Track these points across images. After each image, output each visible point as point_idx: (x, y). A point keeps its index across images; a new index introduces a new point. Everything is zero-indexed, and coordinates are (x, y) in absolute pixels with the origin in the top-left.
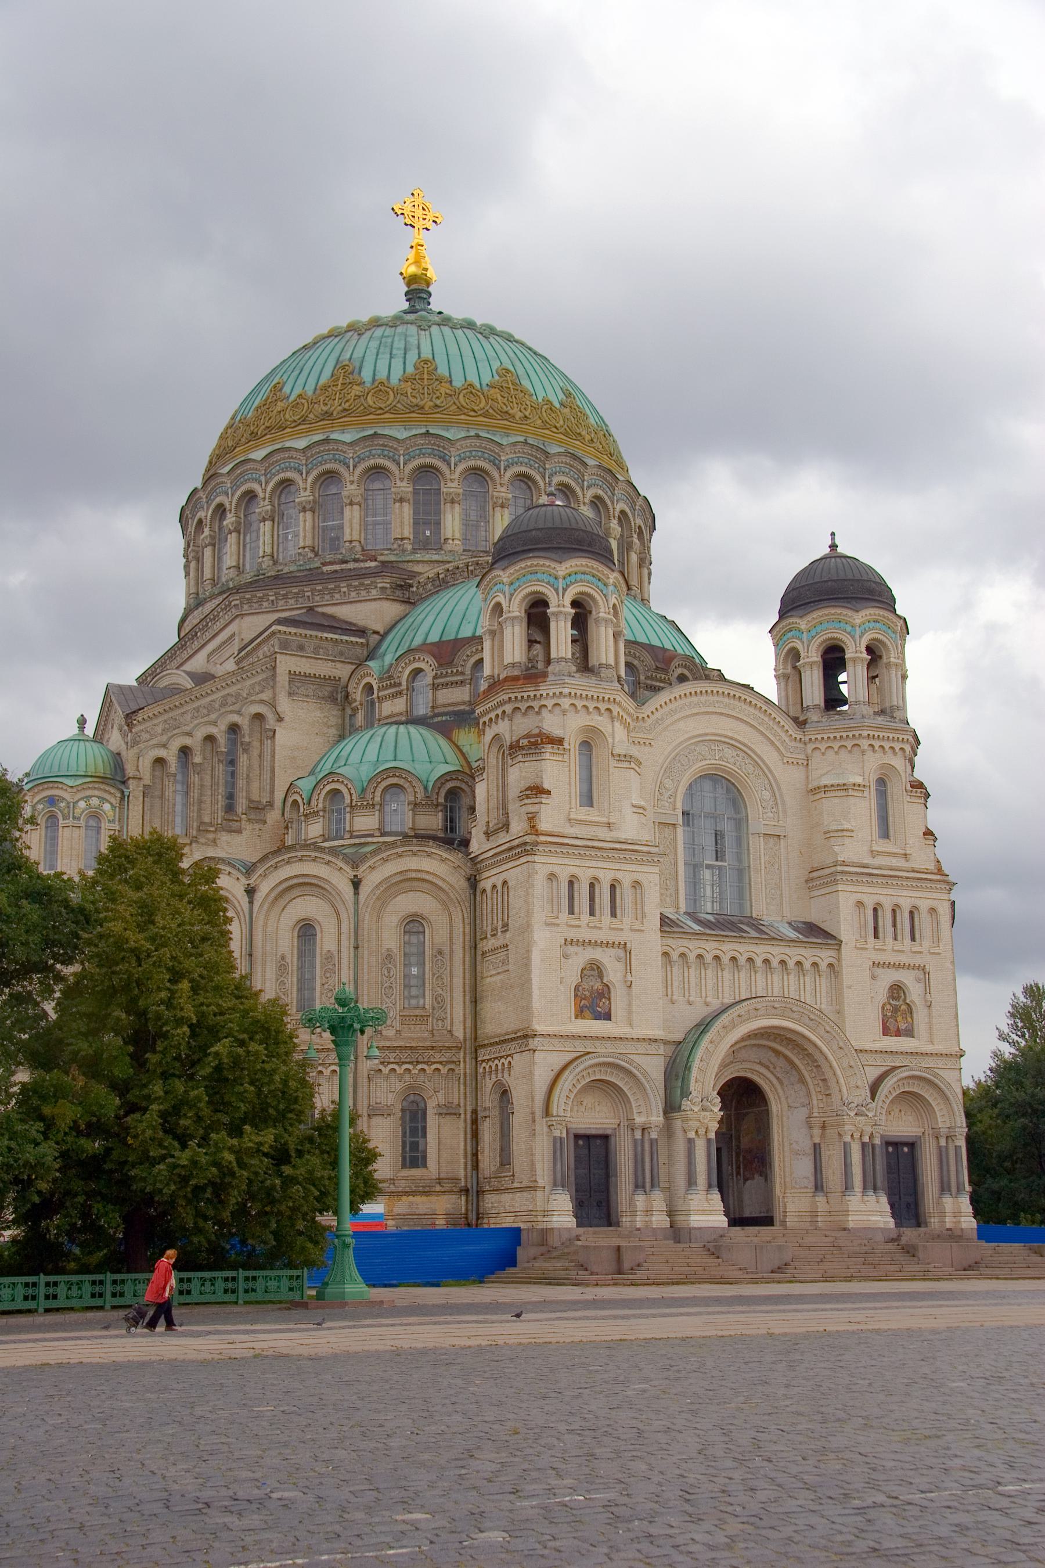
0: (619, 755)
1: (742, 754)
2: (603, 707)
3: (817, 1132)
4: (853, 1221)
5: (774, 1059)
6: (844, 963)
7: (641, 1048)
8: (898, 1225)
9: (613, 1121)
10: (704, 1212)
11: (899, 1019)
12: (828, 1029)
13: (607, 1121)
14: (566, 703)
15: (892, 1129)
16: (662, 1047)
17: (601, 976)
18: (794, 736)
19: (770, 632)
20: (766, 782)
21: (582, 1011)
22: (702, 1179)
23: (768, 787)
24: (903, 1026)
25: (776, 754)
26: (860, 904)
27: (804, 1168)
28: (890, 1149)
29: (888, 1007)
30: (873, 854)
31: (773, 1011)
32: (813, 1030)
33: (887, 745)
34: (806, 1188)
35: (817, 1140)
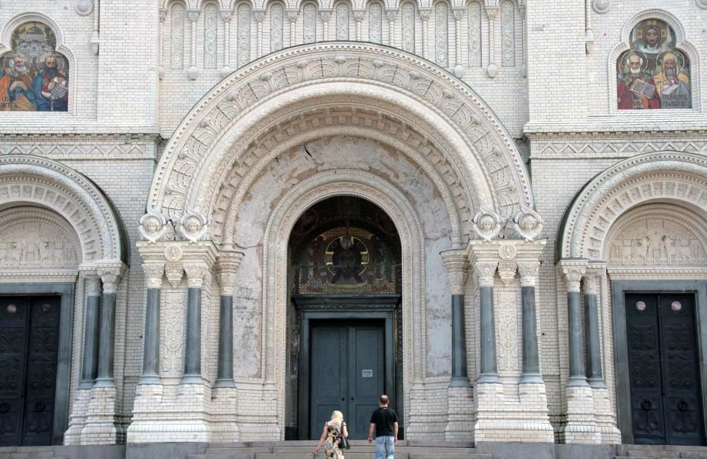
3: (456, 276)
4: (484, 430)
5: (390, 161)
7: (110, 149)
8: (625, 440)
9: (70, 271)
10: (160, 415)
11: (659, 77)
13: (65, 271)
15: (640, 269)
17: (51, 40)
21: (12, 99)
22: (172, 358)
24: (666, 89)
27: (441, 338)
28: (641, 306)
29: (634, 59)
31: (336, 69)
32: (422, 97)
34: (445, 373)
35: (456, 290)
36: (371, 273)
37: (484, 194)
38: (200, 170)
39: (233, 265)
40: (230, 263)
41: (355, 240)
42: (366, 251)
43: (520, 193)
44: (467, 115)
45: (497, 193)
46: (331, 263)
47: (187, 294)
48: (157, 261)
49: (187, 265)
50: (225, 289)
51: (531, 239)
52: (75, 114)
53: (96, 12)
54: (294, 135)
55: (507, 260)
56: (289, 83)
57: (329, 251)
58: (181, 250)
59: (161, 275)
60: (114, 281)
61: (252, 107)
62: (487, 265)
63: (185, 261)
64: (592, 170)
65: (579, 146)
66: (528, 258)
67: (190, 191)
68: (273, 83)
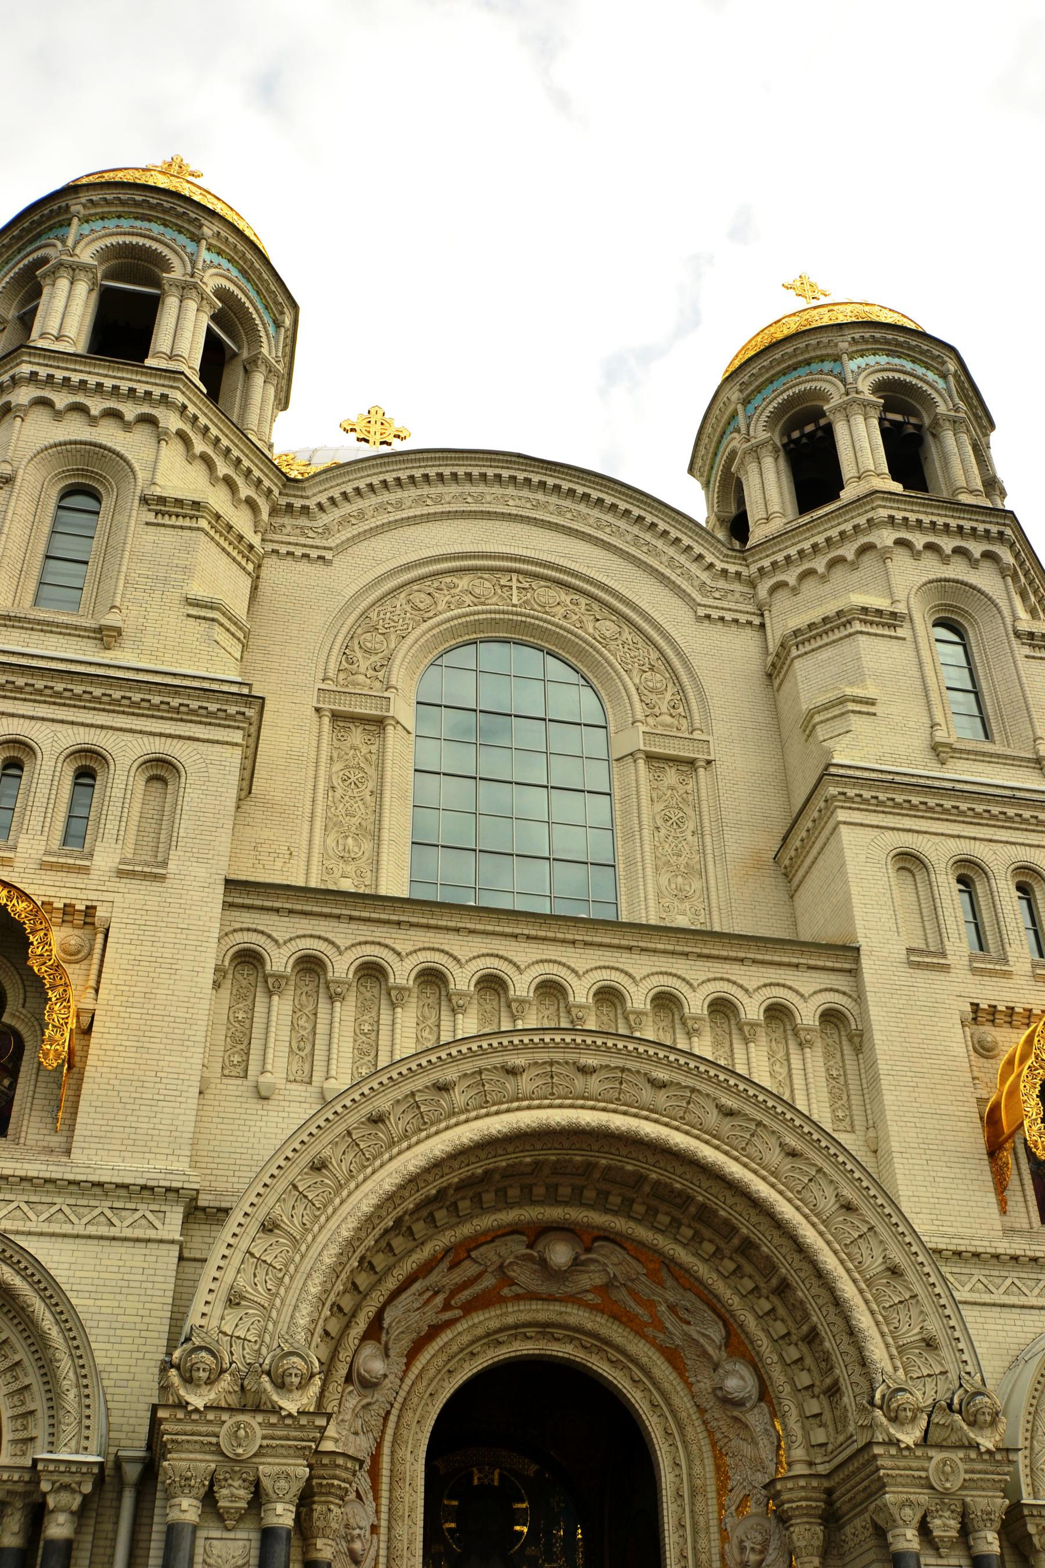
0: (162, 500)
1: (583, 601)
2: (130, 411)
5: (645, 1287)
6: (871, 998)
12: (791, 1141)
14: (23, 395)
16: (175, 1216)
18: (719, 565)
19: (691, 470)
20: (654, 655)
23: (659, 665)
25: (676, 601)
26: (909, 862)
30: (939, 751)
32: (742, 1153)
33: (948, 544)
36: (531, 1551)
37: (878, 1352)
38: (303, 1257)
39: (340, 1487)
40: (336, 1482)
41: (501, 1475)
42: (523, 1502)
43: (946, 1352)
44: (830, 1192)
45: (901, 1349)
46: (453, 1525)
47: (255, 1544)
48: (199, 1456)
49: (266, 1469)
50: (320, 1543)
51: (991, 1447)
52: (22, 1141)
53: (96, 956)
54: (470, 1217)
55: (946, 1493)
56: (487, 1102)
57: (451, 1497)
58: (259, 1432)
59: (202, 1491)
60: (75, 1507)
61: (414, 1139)
62: (910, 1504)
63: (263, 1460)
64: (1025, 1329)
65: (998, 1281)
66: (983, 1489)
67: (278, 1302)
68: (459, 1097)
